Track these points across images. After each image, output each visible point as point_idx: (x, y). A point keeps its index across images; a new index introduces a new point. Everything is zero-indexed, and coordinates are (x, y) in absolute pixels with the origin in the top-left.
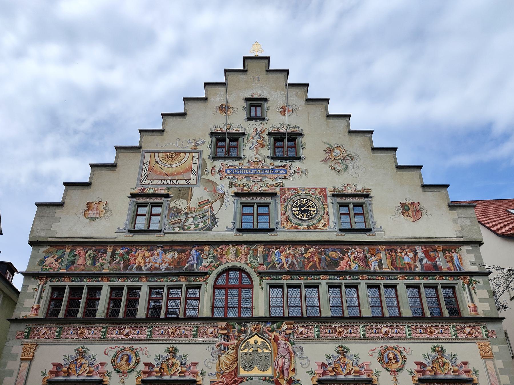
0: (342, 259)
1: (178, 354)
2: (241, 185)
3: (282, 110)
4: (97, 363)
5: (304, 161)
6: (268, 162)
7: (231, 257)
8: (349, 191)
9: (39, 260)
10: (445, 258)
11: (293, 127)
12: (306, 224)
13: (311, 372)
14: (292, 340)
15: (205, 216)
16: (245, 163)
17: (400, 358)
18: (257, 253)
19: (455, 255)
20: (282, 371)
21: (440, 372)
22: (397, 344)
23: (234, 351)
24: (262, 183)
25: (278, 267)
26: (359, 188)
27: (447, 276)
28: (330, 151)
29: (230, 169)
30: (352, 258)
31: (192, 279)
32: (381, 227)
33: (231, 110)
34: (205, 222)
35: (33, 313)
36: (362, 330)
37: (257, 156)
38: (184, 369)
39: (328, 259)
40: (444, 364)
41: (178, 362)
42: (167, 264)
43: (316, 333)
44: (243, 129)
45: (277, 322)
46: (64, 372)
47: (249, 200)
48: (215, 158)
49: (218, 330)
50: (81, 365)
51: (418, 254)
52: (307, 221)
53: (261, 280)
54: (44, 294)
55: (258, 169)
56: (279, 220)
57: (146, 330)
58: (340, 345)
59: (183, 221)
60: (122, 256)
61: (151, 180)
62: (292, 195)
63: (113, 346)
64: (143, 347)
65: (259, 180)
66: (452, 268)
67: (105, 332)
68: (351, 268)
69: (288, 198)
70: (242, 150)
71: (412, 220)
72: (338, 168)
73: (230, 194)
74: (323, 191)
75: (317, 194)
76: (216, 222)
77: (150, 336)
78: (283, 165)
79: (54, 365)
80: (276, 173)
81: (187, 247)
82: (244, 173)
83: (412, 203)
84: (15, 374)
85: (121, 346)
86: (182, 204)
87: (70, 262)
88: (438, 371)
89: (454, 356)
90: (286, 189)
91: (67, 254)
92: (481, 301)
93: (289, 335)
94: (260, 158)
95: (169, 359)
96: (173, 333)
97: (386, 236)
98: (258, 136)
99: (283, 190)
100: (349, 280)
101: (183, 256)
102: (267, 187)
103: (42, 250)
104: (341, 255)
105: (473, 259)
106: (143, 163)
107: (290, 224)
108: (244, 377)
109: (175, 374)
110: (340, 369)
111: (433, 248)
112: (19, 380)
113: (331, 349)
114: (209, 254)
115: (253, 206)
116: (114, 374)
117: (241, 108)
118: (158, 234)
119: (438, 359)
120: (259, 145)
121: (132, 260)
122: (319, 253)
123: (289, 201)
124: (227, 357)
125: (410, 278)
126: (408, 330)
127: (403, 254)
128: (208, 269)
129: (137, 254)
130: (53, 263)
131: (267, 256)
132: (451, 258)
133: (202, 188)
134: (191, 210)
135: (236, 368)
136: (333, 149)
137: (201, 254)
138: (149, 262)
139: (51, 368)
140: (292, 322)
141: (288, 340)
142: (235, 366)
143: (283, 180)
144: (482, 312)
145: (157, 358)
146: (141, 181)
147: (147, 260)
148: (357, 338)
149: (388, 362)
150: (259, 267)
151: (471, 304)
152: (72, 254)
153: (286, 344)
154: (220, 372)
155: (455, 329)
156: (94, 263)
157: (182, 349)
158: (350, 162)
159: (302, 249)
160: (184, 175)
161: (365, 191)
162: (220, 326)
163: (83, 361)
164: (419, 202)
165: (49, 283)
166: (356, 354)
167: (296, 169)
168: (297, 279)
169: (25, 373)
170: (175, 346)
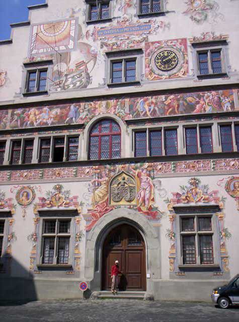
0: (198, 103)
1: (63, 190)
2: (111, 45)
4: (6, 198)
6: (136, 19)
8: (209, 38)
12: (166, 74)
13: (167, 201)
14: (152, 176)
15: (82, 75)
16: (114, 23)
18: (124, 104)
20: (144, 201)
25: (142, 114)
26: (217, 34)
30: (207, 101)
32: (235, 70)
34: (81, 81)
36: (212, 164)
38: (68, 201)
41: (63, 196)
42: (52, 119)
43: (173, 169)
48: (88, 23)
49: (93, 170)
53: (127, 127)
55: (126, 27)
56: (144, 73)
57: (39, 171)
58: (193, 177)
59: (63, 82)
60: (18, 115)
63: (16, 186)
64: (37, 185)
65: (127, 38)
68: (205, 110)
69: (152, 52)
73: (101, 52)
74: (184, 41)
78: (148, 21)
80: (142, 30)
85: (22, 185)
86: (63, 67)
90: (150, 44)
93: (149, 171)
94: (128, 17)
95: (56, 194)
96: (58, 174)
99: (147, 45)
100: (203, 122)
101: (65, 111)
104: (198, 99)
107: (154, 76)
108: (114, 206)
109: (61, 205)
113: (185, 182)
114: (85, 108)
116: (18, 207)
120: (126, 6)
121: (26, 118)
122: (178, 100)
128: (84, 121)
129: (29, 112)
131: (133, 106)
137: (78, 108)
138: (39, 119)
141: (149, 175)
142: (106, 198)
147: (37, 118)
153: (147, 179)
154: (95, 203)
157: (66, 186)
158: (209, 11)
159: (163, 97)
161: (223, 37)
170: (60, 184)
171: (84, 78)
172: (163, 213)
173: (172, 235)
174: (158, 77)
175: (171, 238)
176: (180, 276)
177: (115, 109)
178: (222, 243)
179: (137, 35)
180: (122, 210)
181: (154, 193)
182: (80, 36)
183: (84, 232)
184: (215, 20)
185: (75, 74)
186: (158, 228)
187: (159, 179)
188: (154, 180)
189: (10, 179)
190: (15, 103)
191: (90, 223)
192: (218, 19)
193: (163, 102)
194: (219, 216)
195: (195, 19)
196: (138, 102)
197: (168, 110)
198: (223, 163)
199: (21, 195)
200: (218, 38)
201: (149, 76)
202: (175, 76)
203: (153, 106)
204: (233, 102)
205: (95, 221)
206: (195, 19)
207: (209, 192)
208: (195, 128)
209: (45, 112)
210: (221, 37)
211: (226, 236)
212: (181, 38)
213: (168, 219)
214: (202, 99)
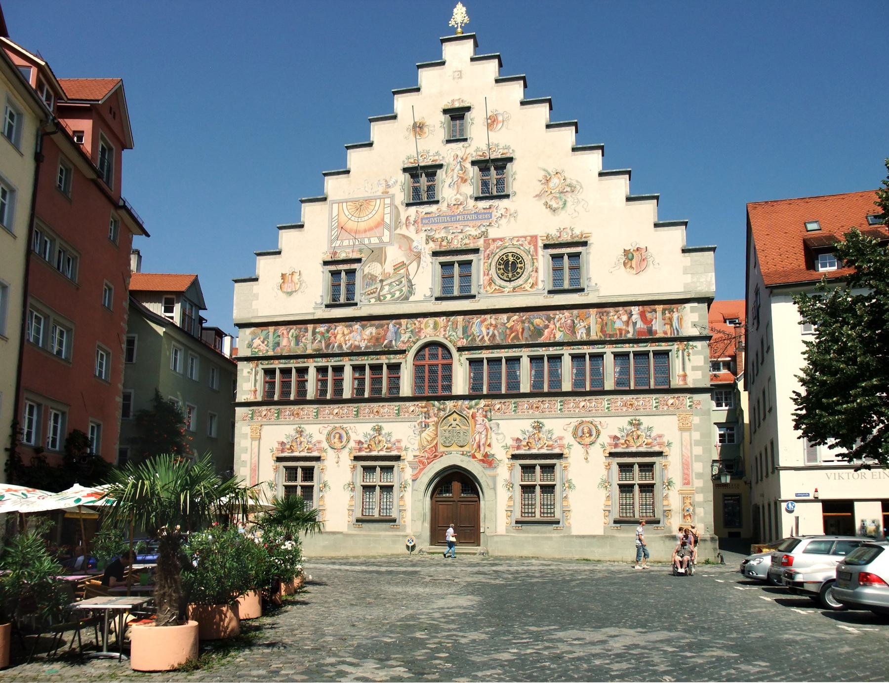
0: (547, 327)
1: (383, 432)
2: (440, 240)
4: (314, 440)
6: (471, 202)
8: (566, 238)
9: (247, 342)
10: (664, 319)
11: (503, 148)
13: (506, 447)
16: (443, 206)
17: (594, 433)
20: (479, 446)
21: (633, 444)
25: (478, 340)
26: (577, 232)
29: (427, 218)
30: (558, 325)
31: (392, 356)
33: (426, 129)
34: (401, 291)
36: (559, 404)
37: (458, 196)
38: (390, 445)
39: (532, 328)
40: (638, 437)
41: (384, 439)
44: (441, 158)
48: (408, 205)
50: (301, 443)
51: (633, 316)
53: (460, 355)
54: (258, 377)
55: (459, 214)
56: (481, 283)
60: (322, 334)
61: (342, 241)
62: (498, 248)
63: (326, 426)
64: (352, 425)
68: (555, 338)
69: (492, 253)
72: (555, 205)
73: (427, 252)
74: (534, 239)
77: (357, 415)
84: (249, 450)
85: (332, 425)
89: (650, 429)
91: (271, 334)
92: (694, 368)
94: (461, 198)
98: (458, 167)
99: (487, 243)
100: (552, 351)
102: (469, 239)
105: (696, 319)
106: (331, 219)
109: (381, 450)
110: (534, 443)
112: (253, 456)
113: (527, 425)
114: (407, 329)
115: (453, 265)
116: (329, 450)
119: (633, 432)
120: (460, 180)
121: (332, 338)
122: (523, 322)
124: (429, 432)
125: (619, 345)
127: (616, 317)
129: (336, 331)
131: (467, 327)
132: (671, 319)
133: (396, 246)
135: (437, 444)
137: (399, 328)
139: (276, 446)
141: (486, 416)
142: (435, 442)
143: (488, 228)
144: (692, 382)
145: (365, 436)
146: (332, 242)
147: (347, 338)
149: (581, 436)
151: (681, 373)
152: (276, 335)
153: (483, 420)
154: (422, 448)
156: (297, 344)
157: (387, 428)
158: (569, 195)
160: (375, 230)
162: (420, 405)
163: (302, 439)
165: (261, 366)
167: (503, 211)
168: (498, 353)
169: (257, 449)
170: (380, 424)
173: (510, 486)
177: (445, 331)
178: (564, 495)
180: (454, 458)
181: (491, 438)
182: (398, 224)
183: (410, 482)
185: (392, 280)
186: (494, 478)
189: (317, 416)
190: (315, 318)
191: (416, 472)
193: (505, 324)
195: (550, 207)
197: (510, 335)
198: (572, 404)
201: (488, 287)
202: (521, 288)
203: (492, 329)
204: (589, 328)
205: (422, 469)
206: (550, 207)
209: (357, 332)
211: (570, 487)
213: (506, 468)
214: (552, 322)
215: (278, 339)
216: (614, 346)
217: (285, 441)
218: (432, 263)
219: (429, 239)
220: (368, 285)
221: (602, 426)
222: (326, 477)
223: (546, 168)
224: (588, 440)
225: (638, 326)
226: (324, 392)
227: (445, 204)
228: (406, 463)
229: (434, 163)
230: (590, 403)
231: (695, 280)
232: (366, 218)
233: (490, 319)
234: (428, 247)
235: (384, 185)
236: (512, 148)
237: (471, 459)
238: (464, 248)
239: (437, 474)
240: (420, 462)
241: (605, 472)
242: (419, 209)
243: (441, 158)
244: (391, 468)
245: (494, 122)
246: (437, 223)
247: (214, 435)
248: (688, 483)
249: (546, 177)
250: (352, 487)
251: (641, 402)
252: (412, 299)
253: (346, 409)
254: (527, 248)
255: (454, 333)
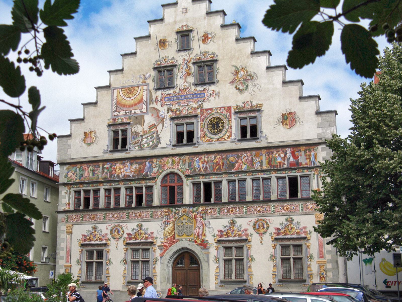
0: (237, 162)
1: (143, 228)
2: (175, 110)
3: (203, 38)
4: (103, 234)
5: (218, 84)
6: (193, 88)
7: (169, 165)
8: (248, 107)
9: (64, 174)
10: (306, 156)
11: (211, 54)
12: (216, 137)
13: (214, 236)
14: (204, 217)
15: (153, 136)
16: (177, 90)
17: (266, 226)
19: (312, 153)
20: (198, 235)
22: (265, 218)
23: (172, 225)
24: (189, 107)
26: (254, 103)
27: (304, 169)
28: (237, 73)
29: (168, 97)
30: (243, 161)
31: (148, 181)
32: (266, 135)
33: (167, 44)
34: (153, 141)
35: (67, 207)
36: (245, 209)
37: (186, 84)
38: (147, 236)
39: (229, 163)
40: (292, 228)
42: (133, 173)
44: (175, 61)
45: (196, 207)
46: (88, 239)
47: (180, 121)
48: (157, 89)
50: (96, 235)
52: (217, 135)
53: (187, 180)
54: (71, 196)
55: (186, 95)
56: (199, 136)
58: (232, 219)
59: (140, 142)
60: (107, 168)
61: (119, 112)
62: (208, 114)
63: (110, 224)
64: (125, 224)
66: (309, 164)
67: (105, 216)
68: (242, 168)
69: (205, 118)
70: (175, 79)
71: (288, 127)
72: (241, 88)
73: (168, 118)
74: (229, 108)
75: (225, 112)
76: (159, 140)
77: (128, 218)
78: (203, 90)
79: (83, 235)
80: (198, 98)
81: (143, 161)
82: (176, 100)
83: (290, 113)
84: (65, 240)
85: (114, 224)
86: (138, 129)
87: (81, 175)
88: (287, 232)
89: (298, 223)
90: (204, 110)
91: (78, 169)
93: (202, 214)
94: (187, 85)
95: (138, 231)
97: (268, 142)
98: (186, 66)
100: (240, 177)
101: (142, 167)
103: (65, 167)
104: (237, 159)
106: (113, 99)
107: (207, 138)
109: (142, 239)
111: (299, 148)
112: (68, 244)
113: (226, 222)
114: (156, 164)
116: (112, 239)
117: (174, 41)
118: (126, 152)
119: (288, 225)
120: (186, 74)
121: (114, 171)
122: (223, 159)
123: (206, 120)
124: (169, 228)
125: (280, 172)
126: (272, 208)
129: (116, 167)
130: (72, 176)
131: (191, 163)
132: (310, 156)
133: (150, 115)
134: (145, 133)
135: (174, 234)
136: (238, 72)
137: (152, 164)
139: (81, 237)
140: (204, 207)
141: (202, 217)
142: (173, 233)
143: (203, 102)
145: (133, 230)
146: (113, 112)
147: (122, 171)
148: (241, 214)
149: (258, 229)
150: (186, 171)
152: (81, 169)
154: (165, 237)
155: (302, 206)
156: (93, 175)
157: (145, 225)
159: (213, 156)
160: (138, 105)
162: (164, 211)
164: (295, 112)
166: (240, 224)
167: (211, 92)
168: (209, 178)
169: (70, 240)
170: (141, 223)
171: (155, 139)
172: (211, 244)
173: (217, 260)
174: (209, 140)
175: (216, 262)
176: (222, 287)
177: (178, 165)
179: (194, 102)
180: (184, 243)
183: (159, 258)
184: (254, 90)
185: (148, 135)
186: (208, 255)
187: (210, 220)
188: (205, 221)
189: (105, 219)
190: (104, 159)
191: (162, 252)
192: (256, 89)
194: (248, 247)
196: (195, 161)
198: (252, 209)
199: (114, 231)
200: (254, 106)
201: (203, 138)
203: (205, 164)
207: (242, 229)
208: (235, 181)
210: (257, 106)
211: (252, 260)
212: (227, 106)
214: (240, 159)
215: (82, 172)
216: (276, 173)
217: (86, 234)
218: (170, 124)
219: (169, 110)
220: (134, 138)
221: (270, 222)
222: (110, 256)
223: (236, 66)
224: (262, 231)
225: (290, 160)
226: (109, 203)
227: (178, 89)
228: (157, 247)
229: (172, 64)
230: (263, 208)
231: (324, 131)
232: (133, 98)
233: (204, 158)
234: (168, 115)
235: (143, 78)
236: (217, 54)
237: (194, 244)
238: (189, 115)
239: (175, 253)
240: (165, 246)
241: (272, 250)
242: (163, 92)
243: (175, 61)
244: (148, 250)
245: (205, 38)
246: (174, 100)
247: (47, 230)
248: (322, 257)
249: (236, 71)
250: (125, 262)
251: (293, 207)
252: (159, 146)
253: (121, 214)
254: (225, 114)
255: (184, 167)
